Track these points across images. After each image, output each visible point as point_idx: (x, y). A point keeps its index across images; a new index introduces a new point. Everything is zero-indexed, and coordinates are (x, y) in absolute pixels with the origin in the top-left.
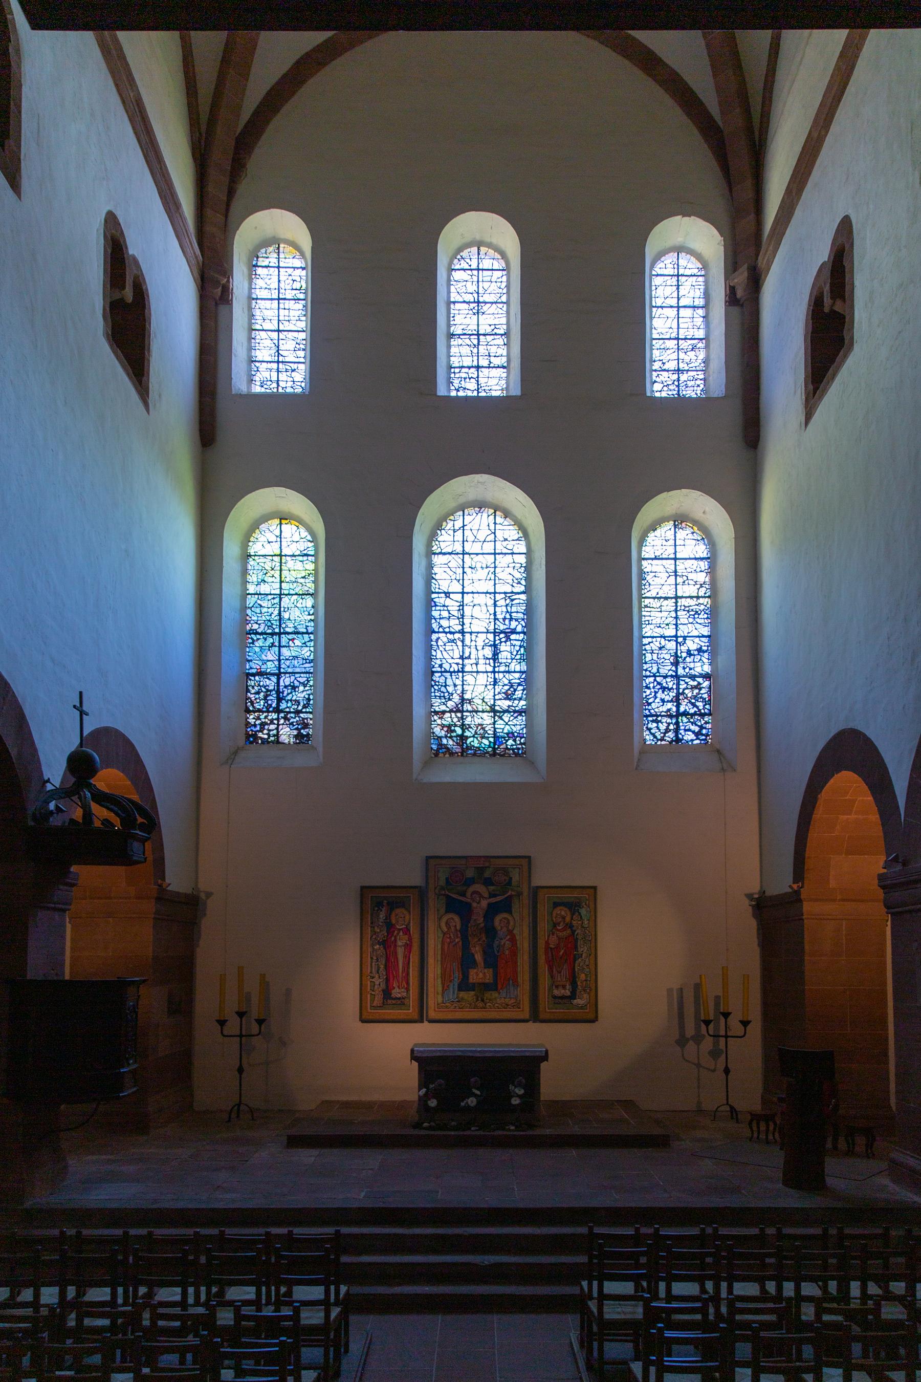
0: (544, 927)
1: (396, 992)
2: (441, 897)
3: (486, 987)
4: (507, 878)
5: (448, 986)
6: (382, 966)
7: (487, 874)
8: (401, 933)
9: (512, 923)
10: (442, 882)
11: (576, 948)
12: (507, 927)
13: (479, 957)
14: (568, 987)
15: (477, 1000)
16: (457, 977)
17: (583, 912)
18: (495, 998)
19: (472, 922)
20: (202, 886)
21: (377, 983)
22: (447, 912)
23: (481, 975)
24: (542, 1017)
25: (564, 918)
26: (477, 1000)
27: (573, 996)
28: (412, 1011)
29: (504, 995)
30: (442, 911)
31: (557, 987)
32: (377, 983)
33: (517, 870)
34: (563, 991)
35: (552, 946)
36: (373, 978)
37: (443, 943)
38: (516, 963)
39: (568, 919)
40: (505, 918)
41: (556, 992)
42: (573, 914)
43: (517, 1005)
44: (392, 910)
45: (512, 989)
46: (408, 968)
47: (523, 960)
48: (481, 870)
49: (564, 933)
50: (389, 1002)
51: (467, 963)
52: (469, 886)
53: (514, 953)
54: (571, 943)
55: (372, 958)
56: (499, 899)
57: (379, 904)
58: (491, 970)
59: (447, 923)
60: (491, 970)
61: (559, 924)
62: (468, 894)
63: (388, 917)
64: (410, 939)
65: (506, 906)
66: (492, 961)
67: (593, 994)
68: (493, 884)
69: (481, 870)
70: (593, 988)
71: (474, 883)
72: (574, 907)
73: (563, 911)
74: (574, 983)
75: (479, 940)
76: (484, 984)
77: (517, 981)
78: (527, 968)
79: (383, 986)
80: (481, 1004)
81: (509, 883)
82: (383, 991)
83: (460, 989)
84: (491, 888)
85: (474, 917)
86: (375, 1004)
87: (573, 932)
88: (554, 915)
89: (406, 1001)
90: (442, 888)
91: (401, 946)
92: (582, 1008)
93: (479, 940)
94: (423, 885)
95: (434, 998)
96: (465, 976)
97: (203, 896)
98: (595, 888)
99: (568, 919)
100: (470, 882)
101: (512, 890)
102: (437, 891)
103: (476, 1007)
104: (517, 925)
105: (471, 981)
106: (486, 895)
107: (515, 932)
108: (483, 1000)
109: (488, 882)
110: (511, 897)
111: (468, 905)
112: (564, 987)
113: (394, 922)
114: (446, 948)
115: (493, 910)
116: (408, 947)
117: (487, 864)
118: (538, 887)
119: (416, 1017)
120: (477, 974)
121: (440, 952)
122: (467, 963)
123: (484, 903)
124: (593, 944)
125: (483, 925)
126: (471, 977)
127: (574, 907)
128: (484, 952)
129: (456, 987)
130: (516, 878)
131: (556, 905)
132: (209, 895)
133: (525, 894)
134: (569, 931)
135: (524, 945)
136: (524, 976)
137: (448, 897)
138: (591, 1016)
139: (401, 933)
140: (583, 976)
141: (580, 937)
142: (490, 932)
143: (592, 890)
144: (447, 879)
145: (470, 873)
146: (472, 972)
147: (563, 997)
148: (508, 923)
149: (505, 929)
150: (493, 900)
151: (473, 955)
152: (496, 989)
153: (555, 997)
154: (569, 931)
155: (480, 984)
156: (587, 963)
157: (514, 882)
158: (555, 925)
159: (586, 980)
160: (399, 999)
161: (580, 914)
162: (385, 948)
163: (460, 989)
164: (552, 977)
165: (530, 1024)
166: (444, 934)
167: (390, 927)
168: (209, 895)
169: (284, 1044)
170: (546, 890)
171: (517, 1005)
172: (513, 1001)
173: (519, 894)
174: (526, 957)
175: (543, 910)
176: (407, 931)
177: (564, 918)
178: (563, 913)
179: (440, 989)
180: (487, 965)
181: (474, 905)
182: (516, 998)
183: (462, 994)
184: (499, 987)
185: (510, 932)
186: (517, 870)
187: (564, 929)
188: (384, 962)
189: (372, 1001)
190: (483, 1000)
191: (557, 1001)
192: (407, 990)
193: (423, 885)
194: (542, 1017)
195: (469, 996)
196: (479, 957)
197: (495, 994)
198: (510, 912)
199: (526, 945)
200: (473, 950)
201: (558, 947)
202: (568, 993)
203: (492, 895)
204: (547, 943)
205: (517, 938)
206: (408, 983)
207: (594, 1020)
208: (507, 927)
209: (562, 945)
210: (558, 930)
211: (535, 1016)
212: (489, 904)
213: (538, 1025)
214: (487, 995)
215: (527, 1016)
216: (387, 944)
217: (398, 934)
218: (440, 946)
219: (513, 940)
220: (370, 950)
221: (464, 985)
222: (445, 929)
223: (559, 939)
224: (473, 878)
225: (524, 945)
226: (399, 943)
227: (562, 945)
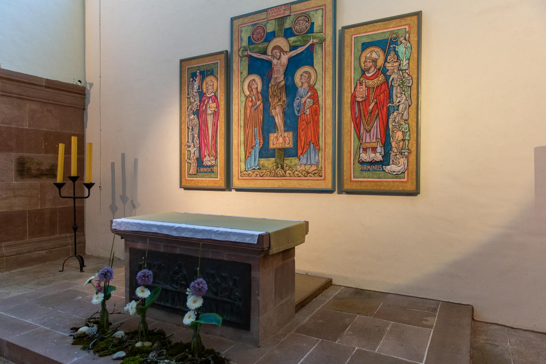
0: (351, 74)
1: (208, 161)
2: (244, 59)
3: (285, 153)
4: (308, 25)
5: (250, 153)
6: (196, 136)
7: (288, 24)
8: (211, 102)
9: (313, 78)
10: (245, 43)
11: (390, 97)
12: (309, 82)
13: (279, 120)
14: (379, 149)
15: (277, 168)
16: (258, 143)
17: (401, 49)
18: (296, 165)
19: (272, 82)
20: (88, 80)
21: (192, 151)
22: (250, 73)
23: (281, 140)
24: (347, 186)
25: (375, 61)
26: (277, 168)
27: (386, 161)
28: (220, 180)
29: (304, 161)
30: (245, 72)
31: (365, 150)
32: (192, 151)
33: (320, 12)
34: (372, 155)
35: (359, 99)
36: (189, 147)
37: (245, 108)
38: (317, 123)
39: (380, 62)
40: (306, 72)
41: (364, 157)
42: (386, 55)
43: (318, 173)
44: (202, 81)
45: (313, 155)
46: (216, 136)
47: (326, 119)
48: (281, 20)
49: (376, 80)
50: (202, 170)
51: (267, 127)
52: (270, 41)
53: (315, 112)
54: (385, 91)
55: (188, 128)
56: (300, 50)
57: (194, 75)
58: (291, 134)
59: (249, 86)
60: (291, 134)
61: (368, 70)
62: (269, 51)
63: (200, 87)
64: (218, 107)
65: (305, 59)
66: (292, 123)
67: (413, 157)
68: (295, 35)
69: (281, 20)
70: (413, 149)
71: (275, 37)
72: (388, 45)
73: (376, 53)
74: (386, 143)
75: (280, 100)
76: (284, 149)
77: (318, 145)
78: (329, 128)
79: (197, 154)
80: (281, 172)
81: (311, 30)
82: (197, 159)
83: (261, 156)
84: (292, 39)
85: (274, 76)
86: (191, 172)
87: (387, 78)
88: (363, 60)
89: (215, 168)
90: (245, 50)
91: (210, 115)
92: (397, 176)
93: (280, 100)
94: (228, 48)
95: (238, 166)
96: (266, 140)
97: (88, 87)
98: (418, 15)
99: (380, 62)
100: (273, 35)
101: (314, 38)
102: (240, 53)
103: (276, 175)
104: (319, 77)
105: (271, 146)
106: (286, 48)
107: (316, 87)
108: (282, 168)
109: (288, 33)
110: (312, 45)
111: (270, 63)
112: (374, 149)
113: (205, 91)
114: (248, 112)
115: (294, 64)
116: (216, 114)
117: (287, 13)
118: (344, 28)
119: (223, 185)
120: (278, 140)
121: (242, 118)
122: (267, 127)
123: (285, 59)
124: (414, 92)
125: (283, 83)
126: (271, 142)
127: (388, 45)
128: (284, 113)
129: (258, 151)
130: (318, 20)
131: (365, 46)
132: (91, 85)
133: (329, 39)
134: (381, 78)
135: (327, 101)
136: (327, 139)
137: (250, 57)
138: (410, 187)
139: (211, 102)
140: (399, 135)
141: (395, 84)
142: (291, 90)
143: (415, 18)
144: (249, 38)
145: (270, 28)
146: (272, 136)
147: (372, 163)
148: (310, 77)
149: (306, 85)
150: (294, 53)
151: (273, 117)
152: (296, 155)
153: (362, 163)
154: (381, 78)
155: (280, 149)
156: (405, 117)
157: (316, 29)
158: (363, 72)
159: (404, 140)
160: (209, 167)
161: (396, 53)
162: (198, 118)
163: (261, 156)
164: (359, 138)
165: (335, 196)
166: (247, 97)
167: (202, 94)
168: (91, 85)
169: (134, 207)
170: (353, 29)
171: (318, 173)
172: (314, 168)
173: (322, 41)
174: (329, 115)
175: (350, 57)
176: (215, 99)
177: (375, 61)
178: (374, 55)
179: (243, 157)
180: (288, 127)
181: (275, 61)
182: (317, 164)
183: (263, 161)
184: (300, 152)
185: (312, 88)
186: (320, 11)
187: (375, 76)
188: (197, 131)
189: (189, 169)
190: (282, 168)
191: (365, 167)
192: (216, 158)
193: (229, 50)
194: (347, 186)
195: (269, 163)
196: (279, 120)
197: (295, 160)
198: (312, 65)
199: (329, 101)
200: (273, 112)
201: (366, 101)
202: (379, 158)
203: (293, 48)
204: (354, 96)
205: (320, 93)
206: (216, 152)
207: (415, 193)
208: (309, 82)
209: (372, 96)
210: (368, 78)
211: (340, 187)
212: (290, 60)
213: (344, 196)
214: (287, 162)
215: (329, 186)
216: (199, 113)
217: (208, 102)
218: (243, 112)
219: (315, 97)
220: (187, 120)
221: (265, 152)
222: (247, 93)
223: (368, 88)
224: (274, 32)
225: (327, 101)
226: (209, 112)
227: (372, 96)
